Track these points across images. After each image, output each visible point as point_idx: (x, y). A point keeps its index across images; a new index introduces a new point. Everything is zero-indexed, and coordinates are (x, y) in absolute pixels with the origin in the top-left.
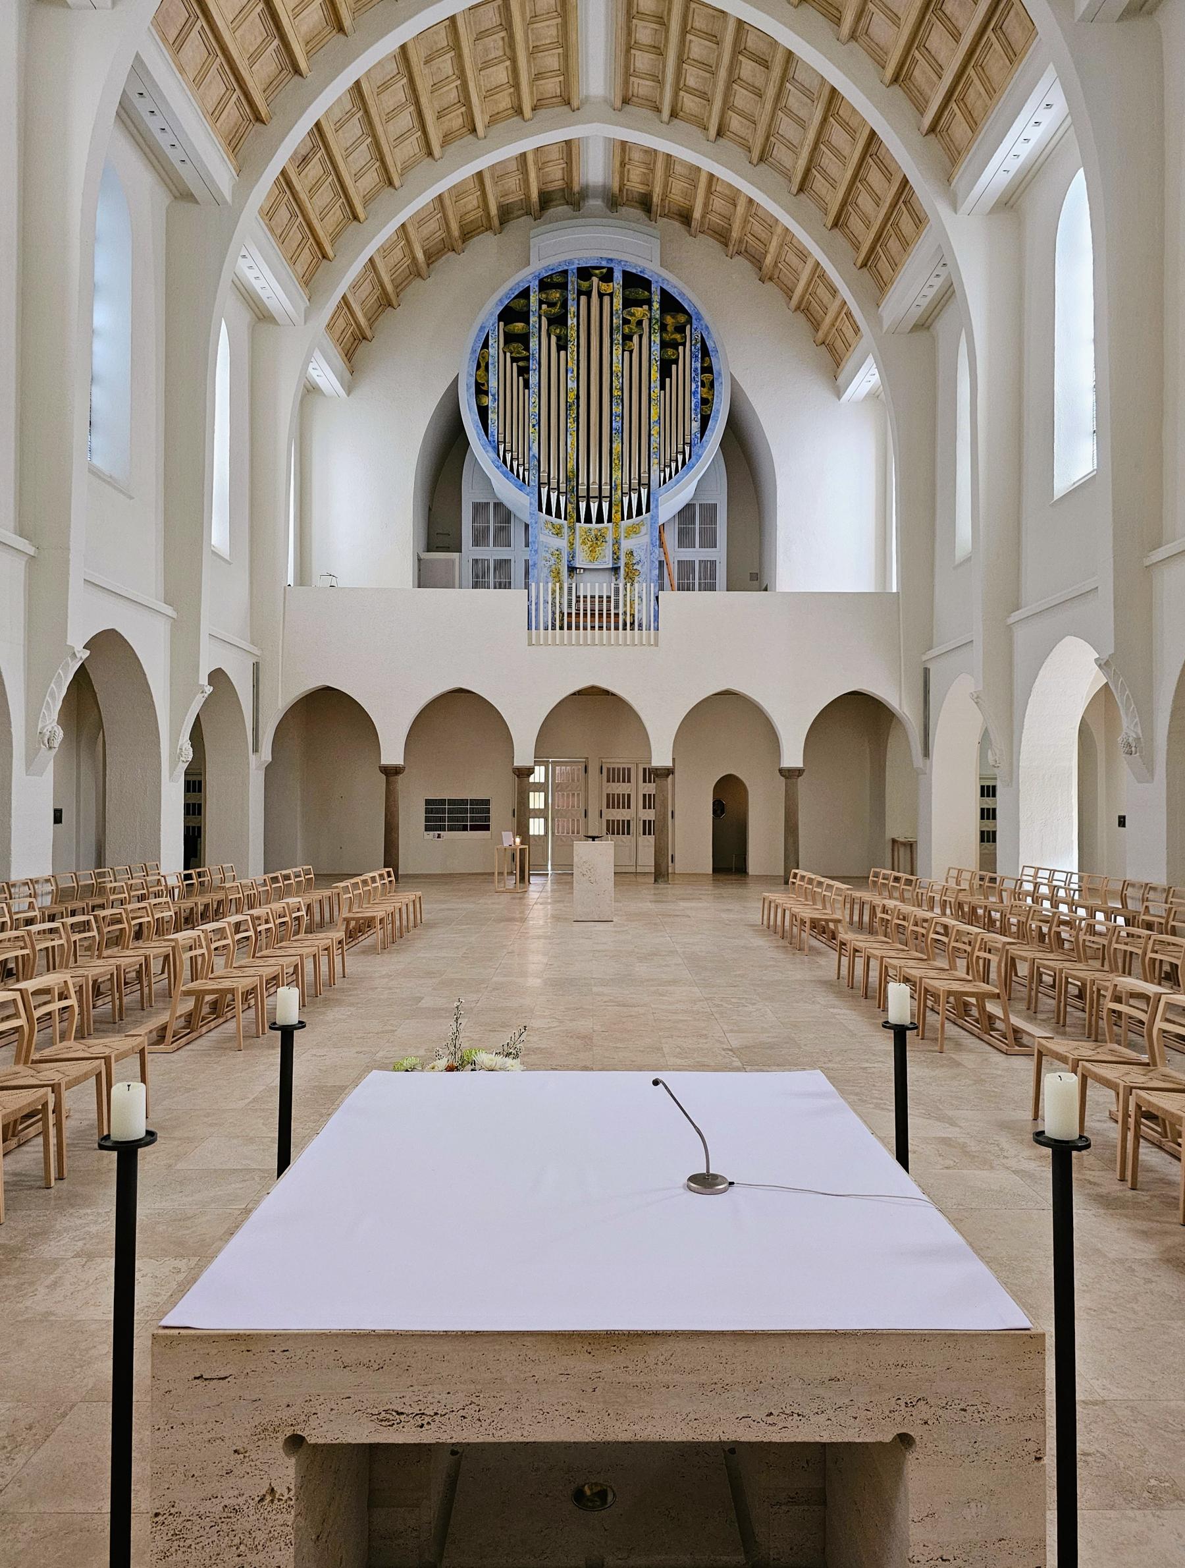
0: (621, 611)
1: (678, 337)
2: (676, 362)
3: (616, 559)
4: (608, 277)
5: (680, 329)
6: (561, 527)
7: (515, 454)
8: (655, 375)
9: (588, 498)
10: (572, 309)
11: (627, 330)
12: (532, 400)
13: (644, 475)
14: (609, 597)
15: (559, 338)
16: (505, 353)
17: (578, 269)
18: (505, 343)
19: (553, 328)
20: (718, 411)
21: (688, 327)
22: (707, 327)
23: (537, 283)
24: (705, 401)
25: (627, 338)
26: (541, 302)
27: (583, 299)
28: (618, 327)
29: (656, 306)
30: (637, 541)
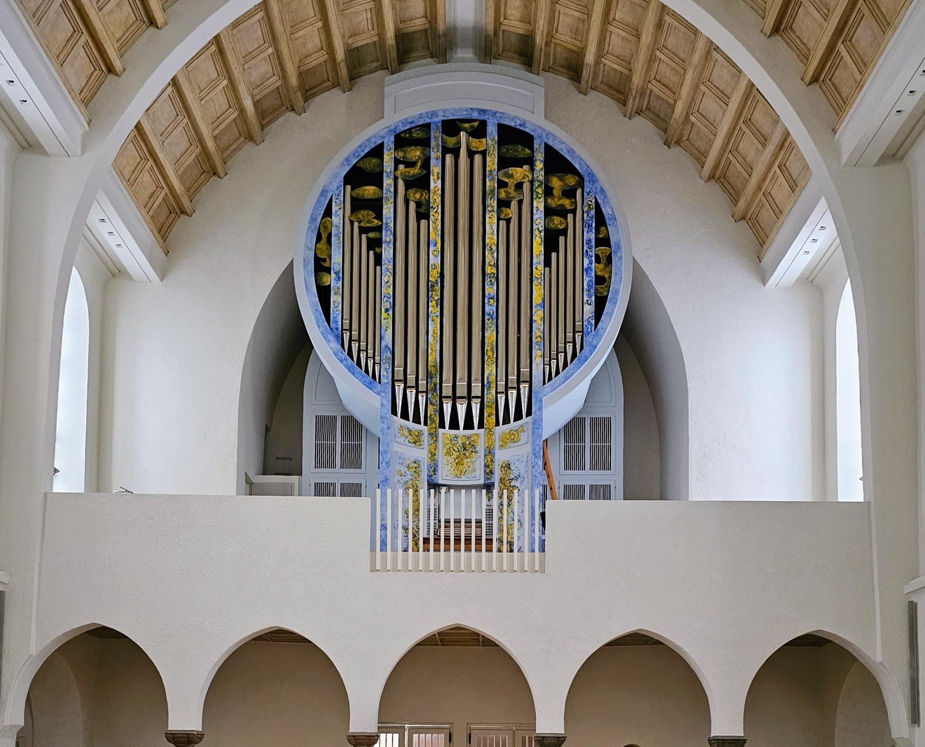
0: (495, 537)
1: (566, 203)
2: (564, 232)
3: (489, 473)
4: (479, 131)
5: (569, 193)
6: (420, 434)
7: (363, 344)
8: (539, 248)
9: (454, 398)
10: (435, 169)
11: (503, 195)
12: (385, 279)
13: (525, 370)
14: (479, 522)
15: (419, 204)
16: (352, 223)
17: (443, 121)
18: (352, 212)
19: (411, 192)
20: (617, 291)
21: (579, 192)
22: (602, 190)
23: (392, 138)
24: (600, 280)
25: (503, 204)
26: (397, 162)
27: (449, 157)
28: (492, 191)
29: (539, 165)
30: (515, 450)
